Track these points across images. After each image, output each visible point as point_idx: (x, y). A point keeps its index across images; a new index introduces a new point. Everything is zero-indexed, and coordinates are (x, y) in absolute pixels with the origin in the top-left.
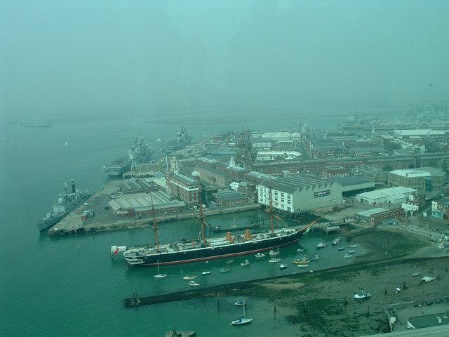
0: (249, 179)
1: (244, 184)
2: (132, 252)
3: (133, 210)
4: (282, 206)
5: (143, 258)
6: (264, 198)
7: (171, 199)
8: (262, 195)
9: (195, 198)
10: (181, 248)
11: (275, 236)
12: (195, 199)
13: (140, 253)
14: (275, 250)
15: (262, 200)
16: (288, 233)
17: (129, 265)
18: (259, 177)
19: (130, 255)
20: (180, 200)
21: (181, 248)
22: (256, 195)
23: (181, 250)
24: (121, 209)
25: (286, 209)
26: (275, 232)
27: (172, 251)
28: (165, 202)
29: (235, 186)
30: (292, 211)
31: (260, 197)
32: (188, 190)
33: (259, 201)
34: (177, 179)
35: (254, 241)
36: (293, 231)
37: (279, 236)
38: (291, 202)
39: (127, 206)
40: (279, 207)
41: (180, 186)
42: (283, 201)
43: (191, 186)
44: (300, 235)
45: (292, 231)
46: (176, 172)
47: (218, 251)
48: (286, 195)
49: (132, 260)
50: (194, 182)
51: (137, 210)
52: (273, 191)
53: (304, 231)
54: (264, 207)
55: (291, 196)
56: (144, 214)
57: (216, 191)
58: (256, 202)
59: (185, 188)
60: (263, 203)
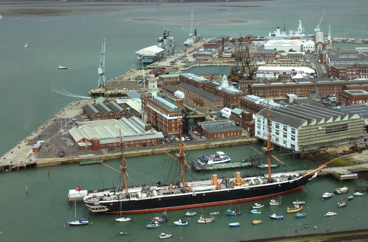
0: (245, 104)
1: (238, 111)
2: (95, 197)
3: (98, 141)
4: (285, 142)
6: (261, 130)
7: (146, 130)
8: (259, 127)
9: (176, 128)
10: (155, 193)
11: (272, 181)
12: (176, 130)
13: (105, 198)
14: (275, 198)
15: (259, 133)
16: (290, 178)
17: (91, 213)
18: (257, 103)
19: (92, 200)
20: (157, 130)
21: (155, 193)
22: (253, 126)
23: (156, 196)
24: (84, 140)
25: (289, 146)
26: (274, 176)
27: (143, 197)
28: (139, 132)
29: (227, 112)
30: (297, 149)
31: (257, 129)
32: (168, 118)
33: (256, 134)
34: (156, 104)
35: (246, 186)
36: (296, 175)
37: (278, 182)
38: (296, 138)
39: (90, 137)
40: (281, 143)
41: (158, 112)
42: (285, 136)
43: (172, 114)
44: (305, 180)
45: (295, 176)
46: (154, 94)
47: (201, 198)
48: (289, 129)
50: (175, 109)
51: (103, 142)
52: (274, 124)
53: (310, 176)
54: (261, 142)
55: (297, 131)
56: (110, 147)
57: (203, 119)
58: (252, 134)
59: (164, 115)
60: (261, 136)
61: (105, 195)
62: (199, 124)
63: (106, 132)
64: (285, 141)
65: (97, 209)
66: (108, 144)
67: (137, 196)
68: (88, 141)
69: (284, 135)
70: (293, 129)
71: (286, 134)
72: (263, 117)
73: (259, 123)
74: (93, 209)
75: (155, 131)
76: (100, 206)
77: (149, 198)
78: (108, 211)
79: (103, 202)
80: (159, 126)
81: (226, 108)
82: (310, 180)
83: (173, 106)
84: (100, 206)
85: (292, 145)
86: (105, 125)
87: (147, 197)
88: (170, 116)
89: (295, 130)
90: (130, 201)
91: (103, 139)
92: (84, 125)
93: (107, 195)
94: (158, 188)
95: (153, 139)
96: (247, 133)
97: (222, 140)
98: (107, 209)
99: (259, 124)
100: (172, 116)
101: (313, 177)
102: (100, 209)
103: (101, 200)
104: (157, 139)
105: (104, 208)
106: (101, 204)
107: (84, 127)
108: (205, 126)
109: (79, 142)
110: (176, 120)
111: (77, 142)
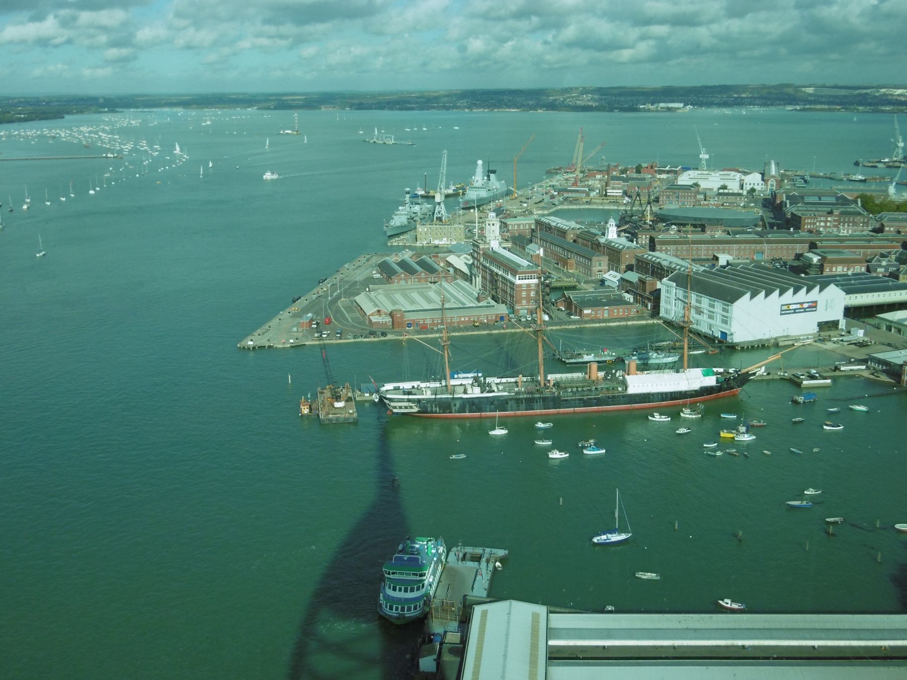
0: (642, 265)
4: (710, 326)
5: (419, 401)
8: (669, 303)
9: (528, 299)
12: (528, 302)
15: (667, 311)
18: (665, 263)
25: (718, 335)
27: (475, 393)
33: (662, 313)
34: (493, 258)
39: (390, 308)
40: (704, 329)
49: (393, 404)
54: (669, 323)
57: (573, 288)
58: (655, 312)
59: (510, 277)
60: (671, 316)
61: (413, 387)
62: (566, 294)
63: (413, 302)
64: (710, 325)
65: (401, 407)
66: (417, 319)
67: (465, 392)
68: (385, 314)
69: (710, 303)
70: (726, 305)
71: (713, 313)
72: (675, 284)
73: (668, 295)
74: (395, 408)
75: (493, 303)
76: (406, 404)
77: (485, 395)
78: (419, 412)
79: (411, 397)
80: (500, 295)
81: (611, 272)
82: (751, 379)
83: (524, 263)
84: (406, 404)
85: (722, 332)
86: (413, 292)
87: (482, 392)
88: (519, 279)
89: (728, 305)
90: (453, 399)
91: (409, 311)
92: (379, 291)
93: (416, 387)
94: (498, 381)
95: (490, 315)
96: (647, 311)
97: (604, 321)
98: (416, 409)
99: (668, 297)
100: (522, 279)
101: (757, 375)
102: (406, 407)
103: (409, 393)
104: (497, 316)
105: (411, 407)
106: (409, 400)
107: (379, 294)
108: (577, 297)
109: (372, 315)
110: (528, 285)
111: (369, 316)
